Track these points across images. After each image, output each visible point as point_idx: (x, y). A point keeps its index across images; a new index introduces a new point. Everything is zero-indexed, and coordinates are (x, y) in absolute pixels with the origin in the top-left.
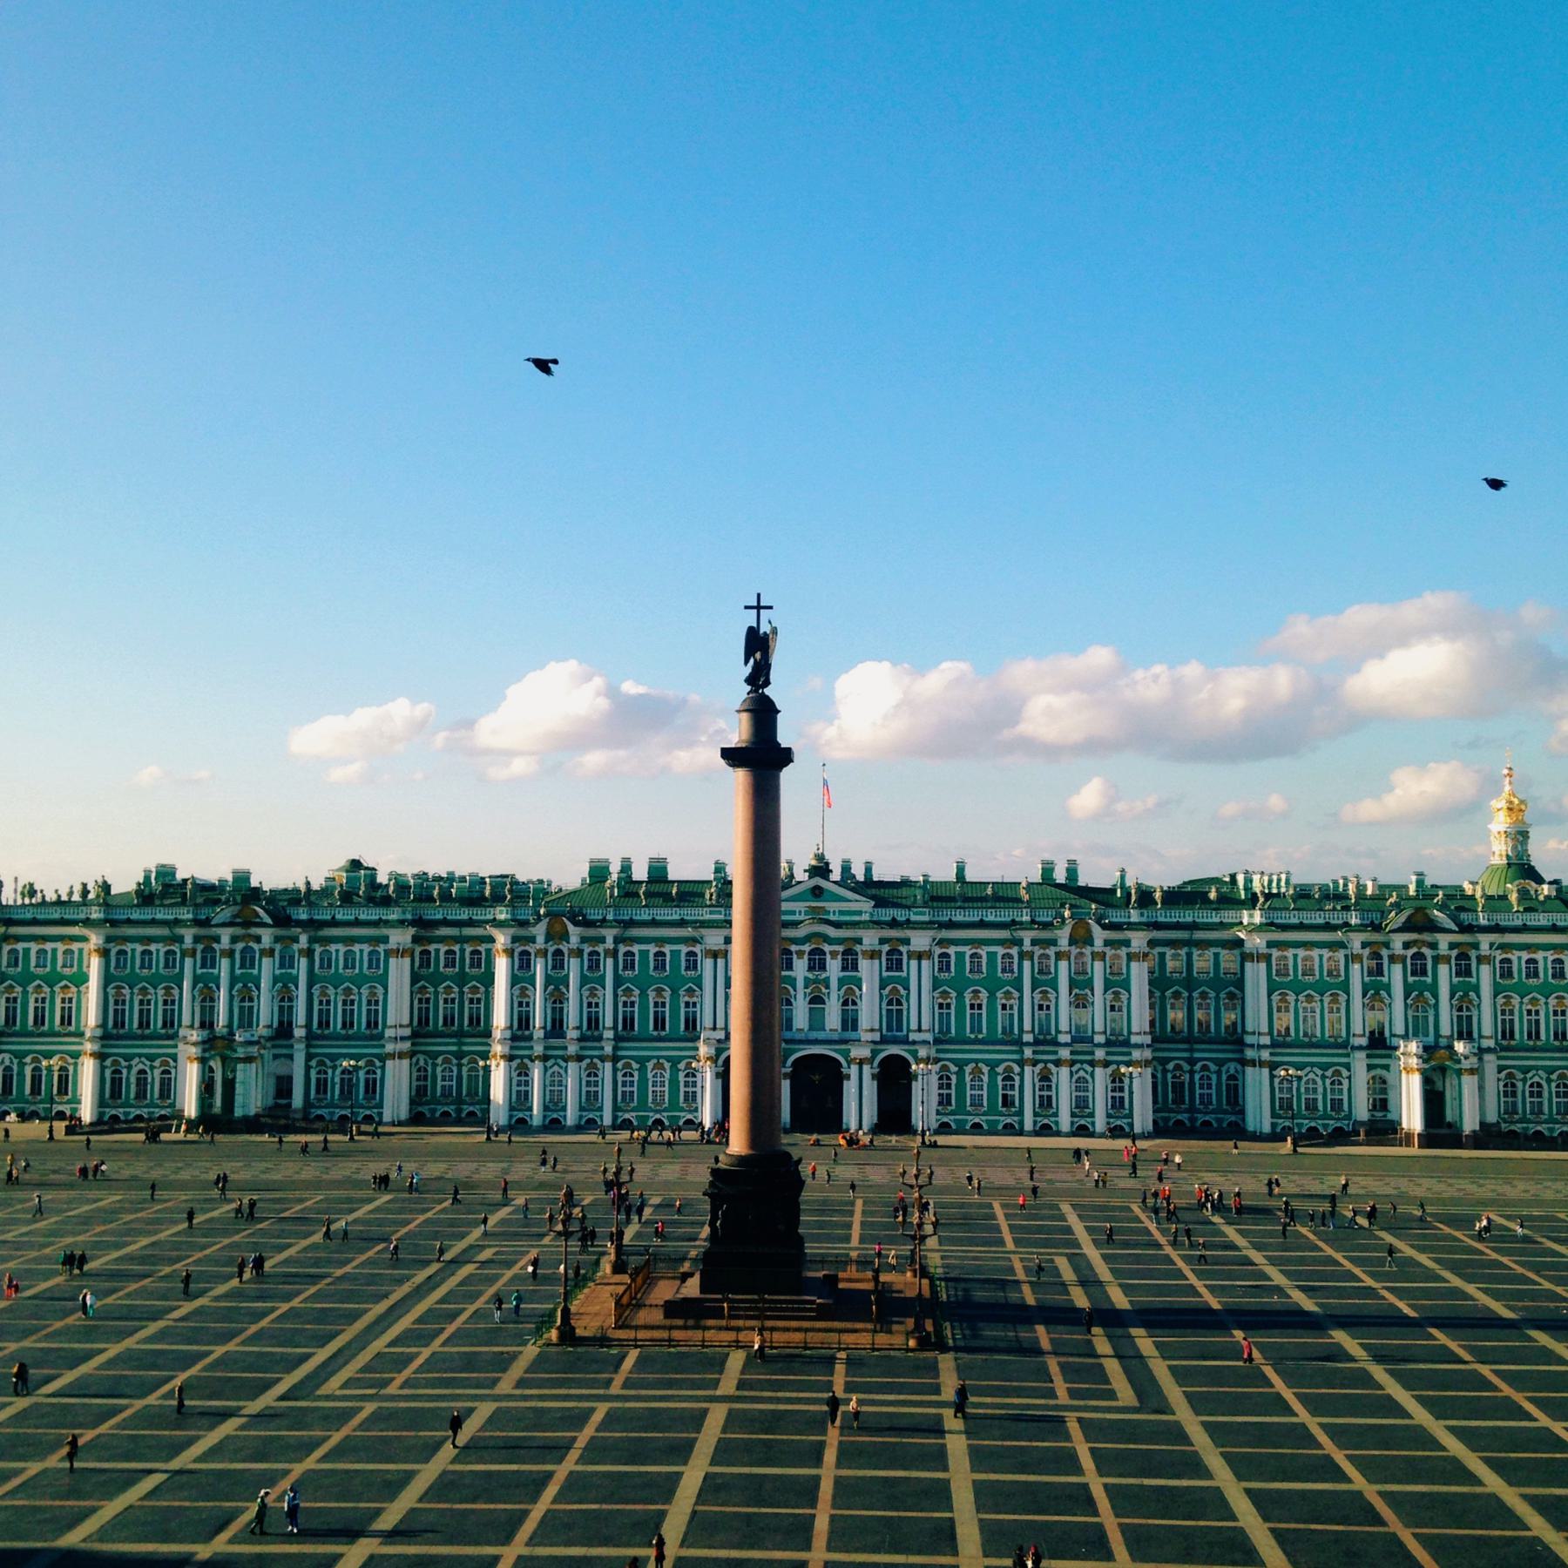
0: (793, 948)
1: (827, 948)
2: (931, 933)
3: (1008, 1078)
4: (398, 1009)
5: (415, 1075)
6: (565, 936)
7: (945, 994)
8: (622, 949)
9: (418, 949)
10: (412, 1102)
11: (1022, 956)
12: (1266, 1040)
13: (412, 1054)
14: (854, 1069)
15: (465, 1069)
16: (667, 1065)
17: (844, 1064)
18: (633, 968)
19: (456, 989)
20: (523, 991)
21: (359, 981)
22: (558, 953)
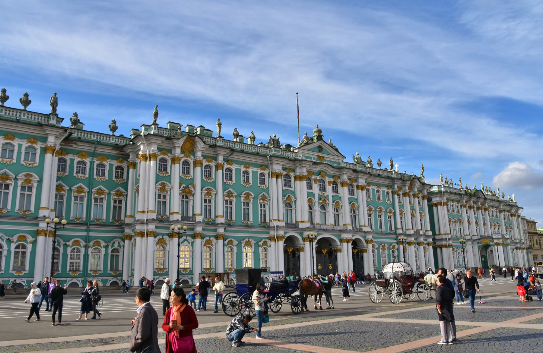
0: (313, 177)
1: (327, 179)
2: (366, 177)
3: (393, 252)
7: (370, 210)
8: (226, 166)
11: (394, 193)
12: (450, 236)
14: (345, 244)
16: (253, 242)
18: (231, 179)
19: (86, 189)
20: (163, 188)
21: (17, 168)
22: (186, 163)
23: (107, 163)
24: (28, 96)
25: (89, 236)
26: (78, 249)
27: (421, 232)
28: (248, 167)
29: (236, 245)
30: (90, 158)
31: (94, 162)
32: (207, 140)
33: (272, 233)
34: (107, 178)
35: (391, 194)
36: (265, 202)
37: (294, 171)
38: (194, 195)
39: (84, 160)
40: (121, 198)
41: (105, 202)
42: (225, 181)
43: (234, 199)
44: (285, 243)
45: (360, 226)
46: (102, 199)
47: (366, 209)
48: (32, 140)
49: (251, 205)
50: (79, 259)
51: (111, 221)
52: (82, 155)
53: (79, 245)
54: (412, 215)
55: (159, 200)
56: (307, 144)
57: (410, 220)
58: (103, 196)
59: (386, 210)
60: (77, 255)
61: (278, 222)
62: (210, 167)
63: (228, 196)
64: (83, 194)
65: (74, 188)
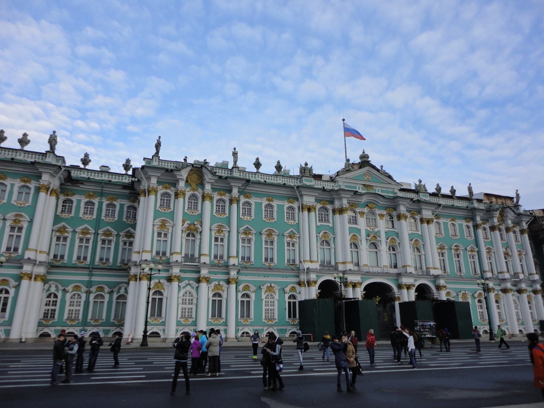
0: (358, 210)
3: (480, 301)
4: (40, 240)
5: (45, 300)
6: (202, 185)
7: (441, 248)
8: (243, 200)
9: (62, 198)
10: (40, 324)
11: (476, 227)
13: (45, 281)
14: (405, 291)
15: (92, 296)
16: (277, 288)
17: (395, 289)
18: (250, 215)
19: (92, 231)
20: (163, 225)
23: (117, 203)
24: (27, 135)
25: (91, 281)
26: (79, 295)
27: (521, 276)
28: (272, 201)
29: (253, 292)
30: (99, 198)
31: (102, 202)
32: (217, 171)
33: (303, 277)
34: (116, 219)
35: (472, 229)
36: (294, 240)
37: (332, 202)
38: (201, 232)
39: (92, 200)
40: (132, 239)
41: (113, 244)
42: (241, 217)
43: (253, 237)
44: (319, 289)
45: (427, 268)
46: (110, 241)
47: (435, 247)
48: (26, 179)
49: (275, 244)
50: (80, 306)
51: (118, 264)
52: (90, 196)
53: (80, 290)
54: (506, 254)
55: (159, 239)
56: (349, 171)
57: (504, 261)
58: (110, 238)
59: (466, 249)
60: (77, 302)
61: (310, 263)
62: (223, 201)
63: (245, 233)
64: (88, 236)
65: (78, 230)
